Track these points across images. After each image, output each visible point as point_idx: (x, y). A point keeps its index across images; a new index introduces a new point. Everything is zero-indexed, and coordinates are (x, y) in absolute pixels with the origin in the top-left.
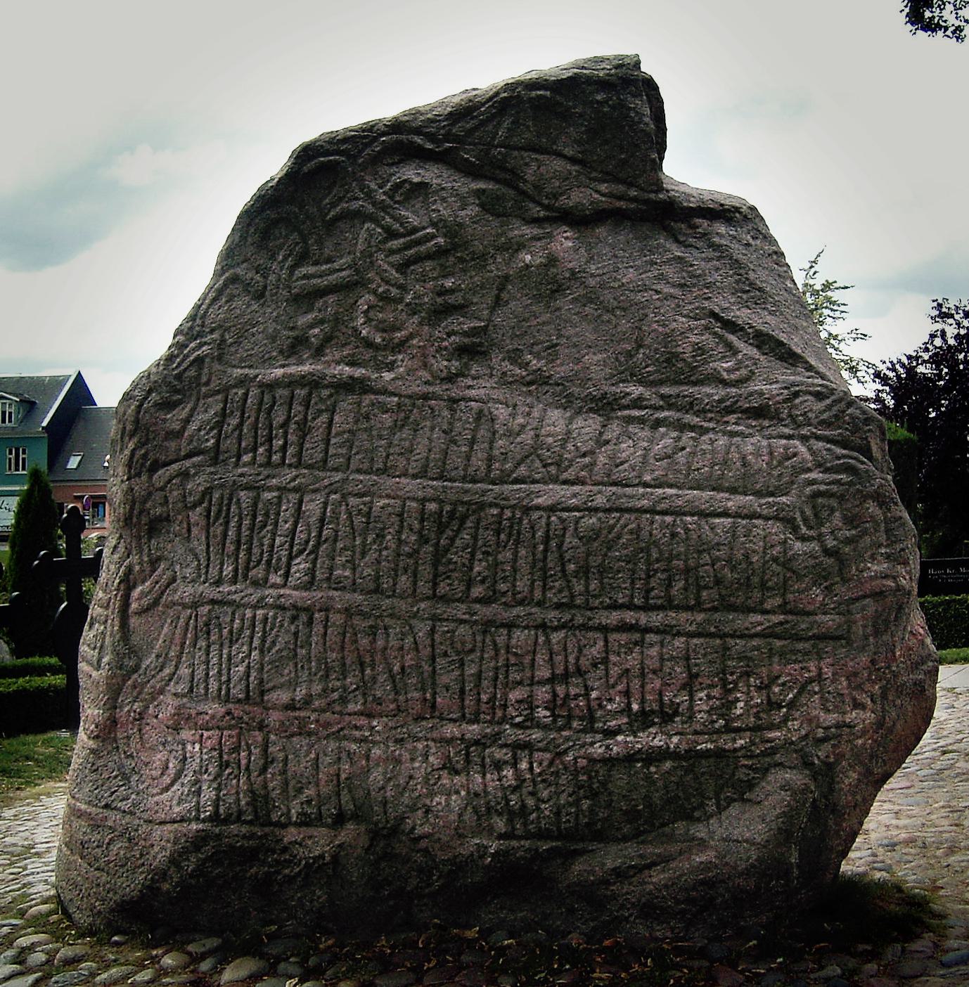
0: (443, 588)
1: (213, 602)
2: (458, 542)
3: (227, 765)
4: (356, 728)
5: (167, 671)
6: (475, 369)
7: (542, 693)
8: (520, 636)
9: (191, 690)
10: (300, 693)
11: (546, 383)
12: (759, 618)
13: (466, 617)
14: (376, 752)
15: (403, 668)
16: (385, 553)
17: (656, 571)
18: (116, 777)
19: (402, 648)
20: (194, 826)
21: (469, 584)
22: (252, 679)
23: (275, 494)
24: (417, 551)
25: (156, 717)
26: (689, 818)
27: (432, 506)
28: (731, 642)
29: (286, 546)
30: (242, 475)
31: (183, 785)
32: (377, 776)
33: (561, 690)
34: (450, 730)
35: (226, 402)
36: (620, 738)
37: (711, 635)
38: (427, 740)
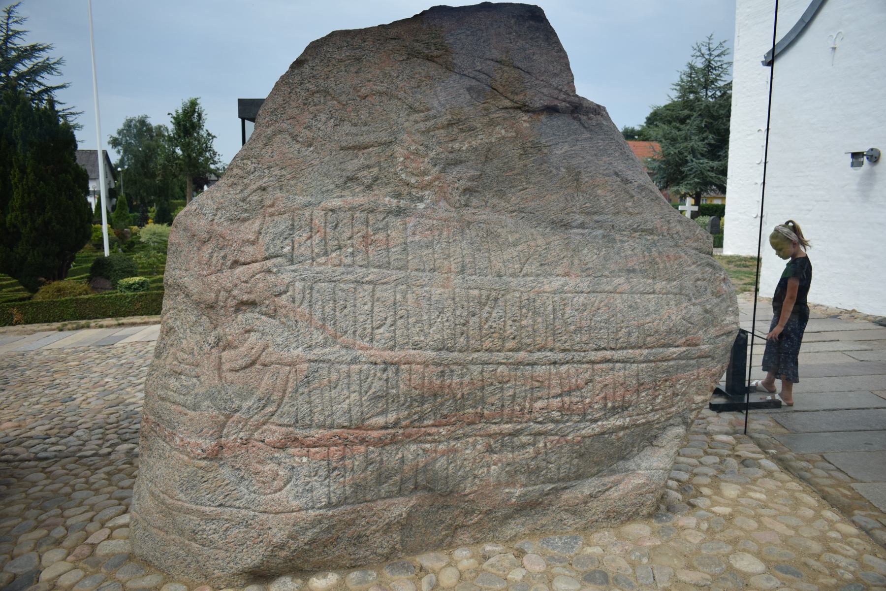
0: (487, 344)
1: (310, 361)
2: (494, 315)
3: (335, 469)
4: (430, 435)
5: (270, 409)
6: (474, 202)
7: (556, 402)
8: (540, 370)
9: (297, 421)
10: (392, 417)
11: (523, 212)
12: (674, 350)
13: (504, 361)
14: (442, 447)
15: (463, 395)
16: (447, 324)
17: (622, 328)
18: (227, 485)
19: (462, 383)
20: (312, 513)
21: (504, 340)
22: (353, 413)
23: (352, 285)
24: (468, 322)
25: (263, 441)
26: (623, 458)
27: (476, 292)
28: (660, 364)
29: (369, 321)
30: (321, 272)
31: (296, 486)
32: (442, 462)
33: (567, 399)
34: (494, 428)
35: (293, 219)
36: (600, 423)
37: (651, 361)
38: (476, 436)
